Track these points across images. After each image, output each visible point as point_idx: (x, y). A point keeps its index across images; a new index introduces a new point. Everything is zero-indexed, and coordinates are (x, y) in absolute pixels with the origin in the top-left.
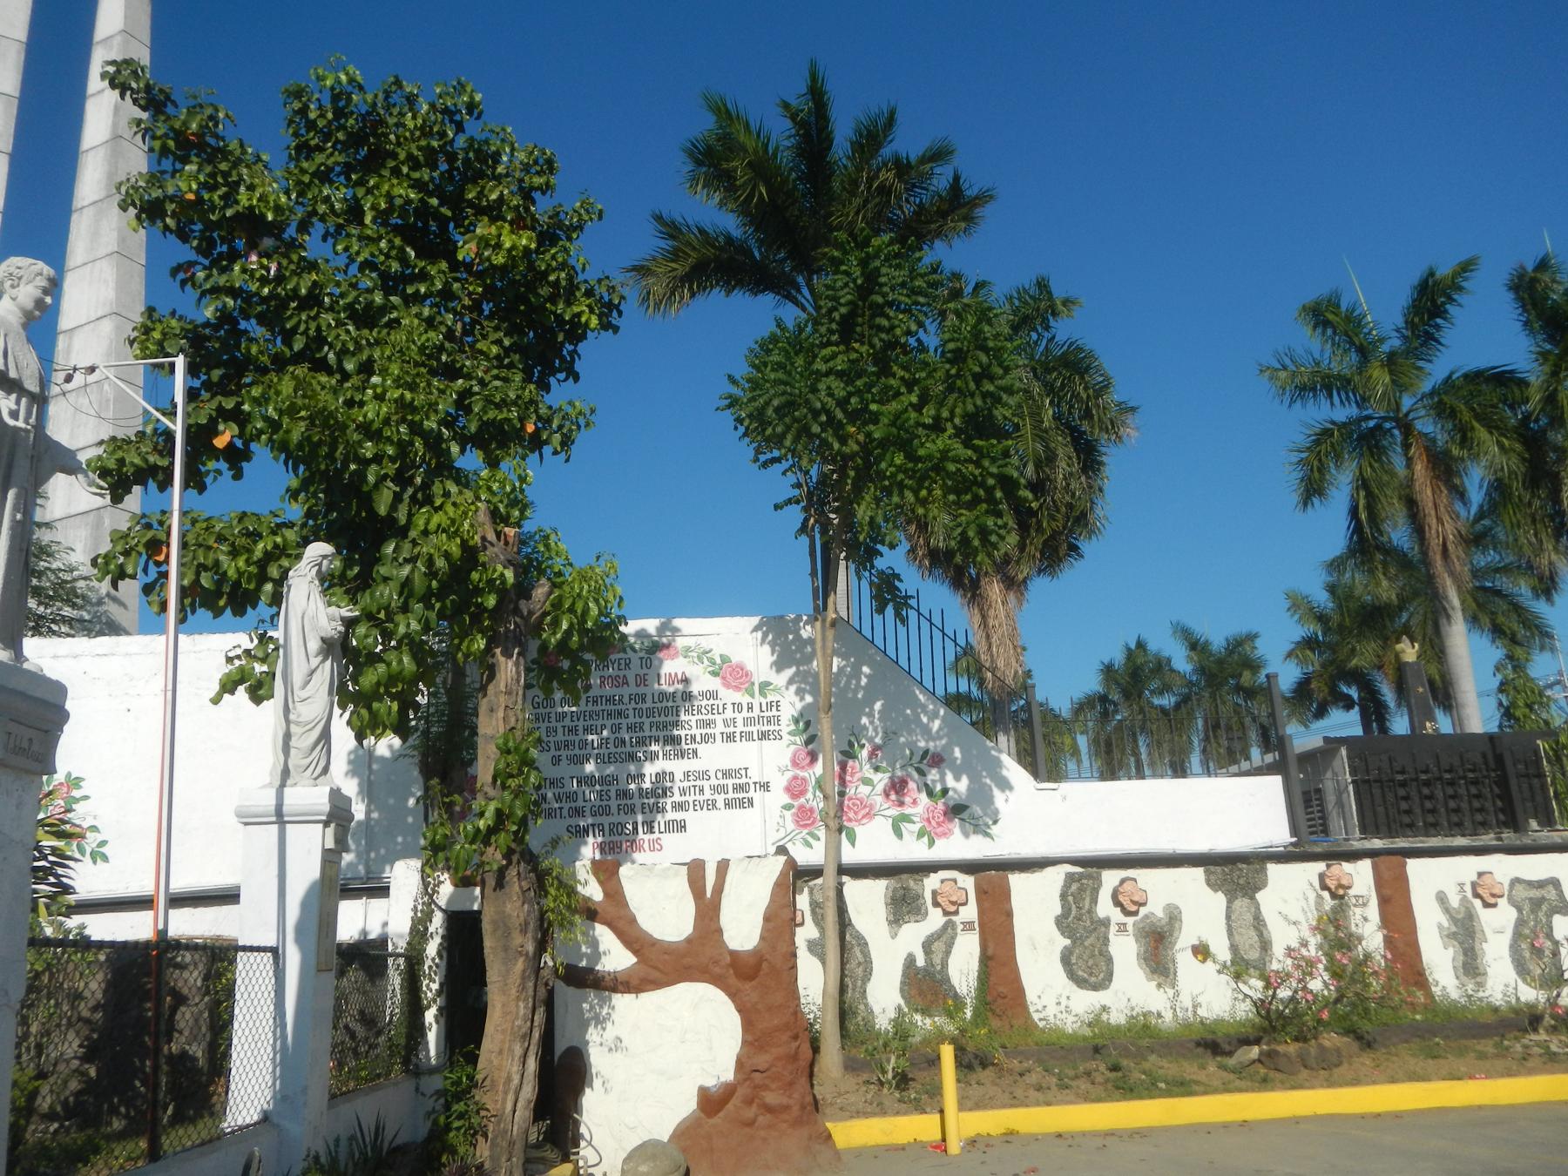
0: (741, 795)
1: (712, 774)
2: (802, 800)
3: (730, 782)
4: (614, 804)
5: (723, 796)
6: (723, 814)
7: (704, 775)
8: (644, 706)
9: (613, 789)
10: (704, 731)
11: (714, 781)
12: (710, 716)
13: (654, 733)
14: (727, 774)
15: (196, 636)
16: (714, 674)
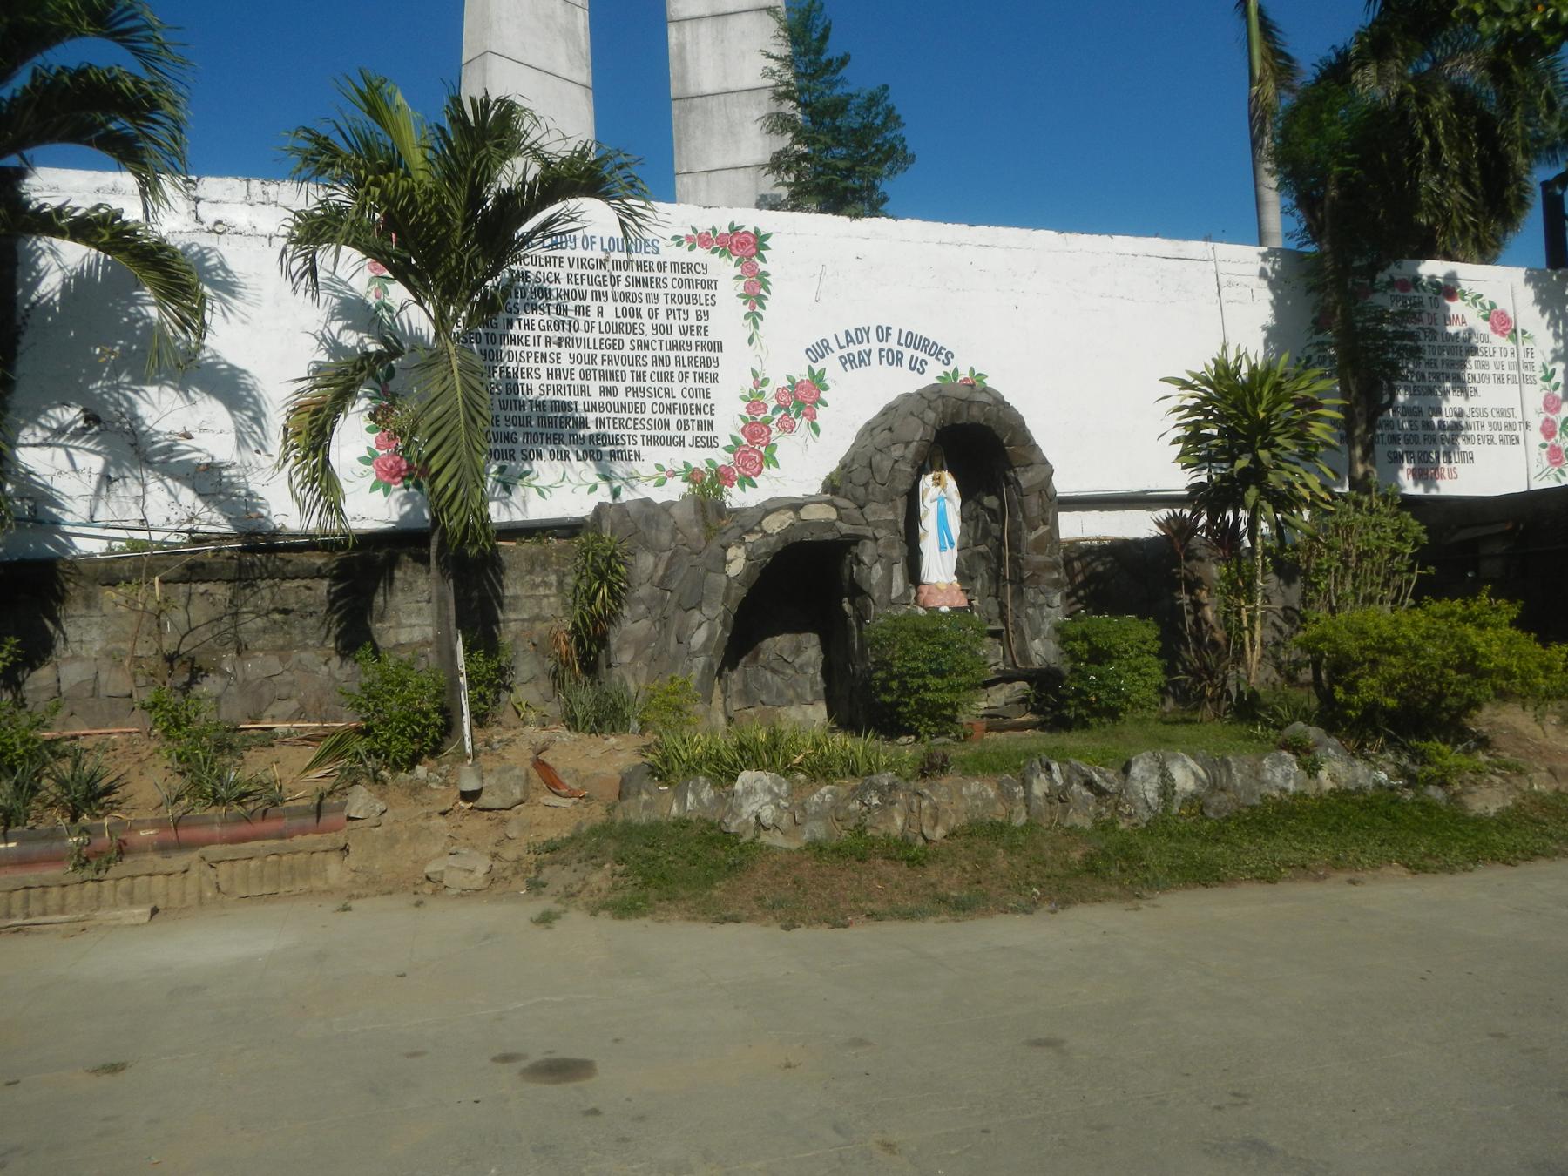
0: (1511, 433)
1: (1489, 411)
2: (1553, 440)
3: (1502, 420)
4: (1421, 433)
5: (1498, 433)
6: (1498, 448)
7: (1483, 412)
8: (1436, 344)
9: (1420, 419)
10: (1481, 372)
11: (1491, 419)
12: (1484, 358)
13: (1445, 370)
14: (1500, 412)
15: (1068, 235)
16: (1486, 318)
